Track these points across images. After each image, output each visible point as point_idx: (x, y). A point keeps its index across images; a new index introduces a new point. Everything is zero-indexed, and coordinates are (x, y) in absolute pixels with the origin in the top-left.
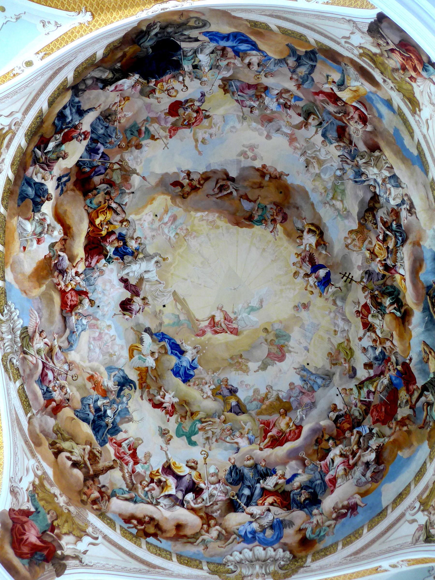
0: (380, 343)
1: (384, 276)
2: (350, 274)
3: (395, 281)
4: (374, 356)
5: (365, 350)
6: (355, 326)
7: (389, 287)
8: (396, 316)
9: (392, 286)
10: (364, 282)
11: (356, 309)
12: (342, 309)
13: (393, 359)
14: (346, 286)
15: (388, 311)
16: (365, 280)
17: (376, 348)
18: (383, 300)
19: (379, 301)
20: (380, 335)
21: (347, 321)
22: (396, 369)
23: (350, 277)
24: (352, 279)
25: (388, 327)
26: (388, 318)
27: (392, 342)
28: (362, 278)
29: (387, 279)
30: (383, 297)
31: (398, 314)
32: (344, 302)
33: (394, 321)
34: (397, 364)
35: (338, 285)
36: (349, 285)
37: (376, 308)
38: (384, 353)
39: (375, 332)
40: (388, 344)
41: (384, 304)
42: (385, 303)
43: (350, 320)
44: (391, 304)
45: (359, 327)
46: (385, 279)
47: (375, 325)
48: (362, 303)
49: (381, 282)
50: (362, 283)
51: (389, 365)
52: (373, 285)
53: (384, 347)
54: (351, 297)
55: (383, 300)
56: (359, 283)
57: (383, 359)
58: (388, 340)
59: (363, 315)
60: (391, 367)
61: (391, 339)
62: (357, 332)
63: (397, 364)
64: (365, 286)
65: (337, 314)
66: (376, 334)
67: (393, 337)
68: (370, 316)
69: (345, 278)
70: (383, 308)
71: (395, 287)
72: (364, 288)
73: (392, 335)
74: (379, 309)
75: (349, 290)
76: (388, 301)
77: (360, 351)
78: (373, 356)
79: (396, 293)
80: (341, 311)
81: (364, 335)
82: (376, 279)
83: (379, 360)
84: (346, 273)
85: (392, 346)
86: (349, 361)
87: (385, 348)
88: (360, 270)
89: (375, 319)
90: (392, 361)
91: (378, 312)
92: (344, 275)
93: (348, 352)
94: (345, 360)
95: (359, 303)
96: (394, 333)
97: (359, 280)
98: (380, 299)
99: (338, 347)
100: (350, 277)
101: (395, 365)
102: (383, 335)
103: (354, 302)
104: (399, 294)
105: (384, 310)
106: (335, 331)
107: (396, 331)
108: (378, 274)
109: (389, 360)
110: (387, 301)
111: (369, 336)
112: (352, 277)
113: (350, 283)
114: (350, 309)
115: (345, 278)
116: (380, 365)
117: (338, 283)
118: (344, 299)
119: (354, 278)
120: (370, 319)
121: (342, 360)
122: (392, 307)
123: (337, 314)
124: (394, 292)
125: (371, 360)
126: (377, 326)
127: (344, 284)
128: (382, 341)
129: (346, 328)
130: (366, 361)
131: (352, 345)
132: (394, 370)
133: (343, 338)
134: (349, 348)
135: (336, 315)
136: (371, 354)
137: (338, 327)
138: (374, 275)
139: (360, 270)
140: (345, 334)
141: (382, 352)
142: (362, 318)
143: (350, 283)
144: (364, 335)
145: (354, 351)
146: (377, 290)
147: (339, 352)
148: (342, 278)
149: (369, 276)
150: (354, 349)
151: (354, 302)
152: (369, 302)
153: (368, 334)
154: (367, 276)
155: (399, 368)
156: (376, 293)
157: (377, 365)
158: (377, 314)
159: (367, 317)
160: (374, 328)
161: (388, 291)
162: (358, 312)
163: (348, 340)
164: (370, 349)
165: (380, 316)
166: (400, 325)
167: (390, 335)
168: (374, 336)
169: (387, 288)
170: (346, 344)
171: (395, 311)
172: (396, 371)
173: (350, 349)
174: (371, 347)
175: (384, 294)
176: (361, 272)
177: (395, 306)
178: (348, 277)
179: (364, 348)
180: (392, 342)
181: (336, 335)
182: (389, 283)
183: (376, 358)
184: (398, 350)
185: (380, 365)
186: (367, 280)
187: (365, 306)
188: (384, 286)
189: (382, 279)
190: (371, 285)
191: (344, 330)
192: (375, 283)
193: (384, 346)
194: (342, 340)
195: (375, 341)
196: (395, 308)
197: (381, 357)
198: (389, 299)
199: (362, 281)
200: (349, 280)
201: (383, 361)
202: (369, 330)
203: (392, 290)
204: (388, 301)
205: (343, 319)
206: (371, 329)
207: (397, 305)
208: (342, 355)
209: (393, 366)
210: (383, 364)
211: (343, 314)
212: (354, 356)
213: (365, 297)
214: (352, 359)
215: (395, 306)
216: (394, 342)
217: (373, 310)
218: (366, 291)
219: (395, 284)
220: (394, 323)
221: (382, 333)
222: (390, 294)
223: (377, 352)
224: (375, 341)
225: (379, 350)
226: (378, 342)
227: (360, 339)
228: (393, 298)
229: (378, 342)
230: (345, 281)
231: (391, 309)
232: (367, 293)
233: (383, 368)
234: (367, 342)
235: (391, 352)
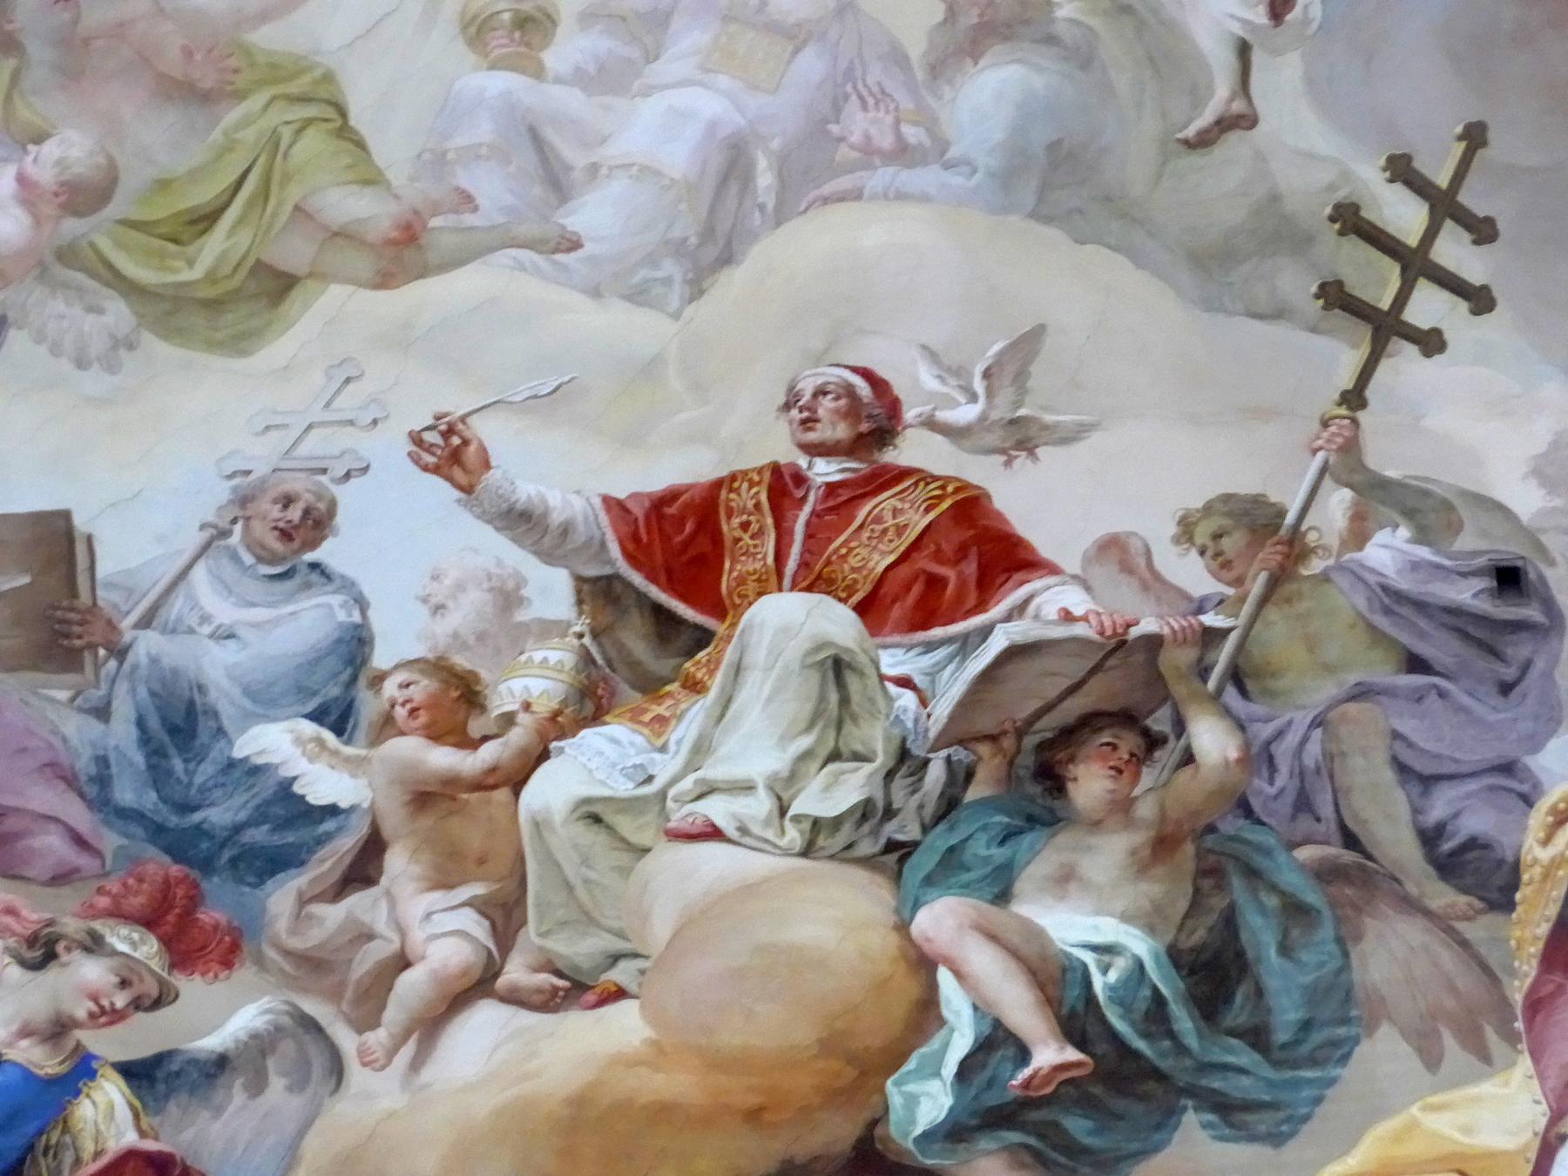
0: (429, 797)
1: (1486, 875)
2: (1480, 300)
3: (1431, 1059)
4: (224, 695)
5: (289, 532)
6: (650, 369)
7: (1318, 952)
8: (893, 1058)
9: (1336, 1022)
10: (1358, 534)
11: (918, 386)
12: (903, 154)
13: (225, 1014)
14: (1275, 230)
15: (942, 919)
16: (1389, 551)
17: (337, 717)
18: (1106, 856)
19: (1090, 784)
20: (552, 790)
21: (713, 233)
22: (83, 1069)
23: (1428, 306)
24: (1386, 328)
25: (700, 921)
26: (838, 920)
27: (480, 984)
28: (1427, 510)
29: (1442, 923)
30: (1163, 845)
31: (923, 1100)
32: (1007, 177)
33: (804, 1034)
34: (142, 1075)
35: (1280, 82)
36: (1296, 284)
37: (958, 733)
38: (277, 862)
39: (589, 703)
40: (437, 928)
41: (1044, 858)
42: (1065, 879)
43: (732, 284)
44: (1060, 986)
45: (632, 439)
46: (1442, 896)
47: (695, 715)
48: (1023, 498)
49: (1393, 835)
50: (1337, 504)
51: (121, 938)
52: (1324, 691)
53: (373, 848)
54: (1091, 299)
55: (1106, 856)
56: (1347, 462)
57: (199, 860)
58: (505, 916)
59: (841, 501)
60: (92, 972)
61: (516, 972)
62: (550, 403)
63: (142, 1075)
64: (1296, 548)
65: (811, 65)
66: (559, 726)
67: (548, 1002)
68: (835, 621)
69: (1405, 216)
70: (980, 848)
71: (1340, 1050)
72: (1254, 534)
73: (575, 989)
74: (959, 778)
75: (1215, 267)
76: (1109, 930)
77: (261, 455)
78: (217, 668)
79: (1246, 1071)
80: (858, 124)
81: (521, 522)
82: (1433, 733)
83: (157, 774)
84: (1483, 231)
85: (411, 986)
86: (67, 255)
87: (363, 870)
88: (1544, 472)
89: (798, 700)
90: (192, 988)
91: (906, 761)
92: (1444, 206)
93: (215, 245)
94: (84, 195)
95: (1021, 439)
96: (624, 1026)
97: (1388, 457)
98: (1122, 807)
99: (278, 71)
100: (1428, 306)
101: (140, 1037)
102: (569, 839)
103: (1027, 345)
104: (1230, 1114)
105: (952, 861)
106: (533, 27)
107: (658, 1055)
108: (1511, 779)
109: (195, 944)
110: (1096, 915)
111: (508, 597)
112: (1431, 342)
113: (1335, 296)
114: (904, 281)
115: (1405, 216)
116: (96, 787)
117: (1319, 90)
118: (1056, 181)
119: (1404, 361)
120: (786, 625)
121: (69, 149)
122: (1022, 1010)
123: (811, 65)
124: (1257, 1037)
125: (147, 645)
126: (685, 732)
127: (1307, 190)
128: (471, 835)
129: (594, 215)
130: (129, 550)
131: (335, 314)
132: (58, 1030)
133: (437, 162)
134: (293, 253)
135: (797, 37)
136: (238, 636)
137: (604, 79)
138: (1487, 708)
139: (1544, 472)
140: (494, 191)
141: (295, 815)
142: (783, 486)
143: (1335, 296)
144: (521, 522)
145: (240, 343)
146: (1259, 758)
147: (194, 92)
148: (1402, 170)
149: (1456, 619)
150: (279, 350)
151: (1027, 345)
152: (1052, 607)
153: (551, 592)
154: (1468, 594)
155: (106, 1115)
156: (1212, 740)
157: (78, 731)
158: (876, 737)
159: (815, 581)
160: (651, 686)
161: (1260, 932)
162: (875, 417)
163: (404, 253)
164: (307, 622)
165: (845, 790)
166: (754, 1116)
167: (579, 949)
168: (531, 682)
169: (1296, 911)
170: (348, 204)
171: (961, 1042)
172: (42, 1060)
173: (275, 287)
174: (355, 645)
175: (1206, 855)
176: (1526, 501)
177: (1049, 1053)
178: (1416, 264)
179: (316, 523)
180: (480, 984)
181: (477, 31)
182: (1393, 954)
183: (180, 723)
184: (373, 1094)
185: (96, 787)
186: (1392, 599)
187: (1001, 558)
188: (1326, 874)
189: (1430, 838)
190: (1320, 660)
191: (558, 183)
192: (1365, 731)
193: (398, 862)
194: (393, 148)
195: (457, 701)
196: (998, 1042)
197: (219, 815)
198: (1139, 944)
199: (1380, 497)
200: (1378, 281)
201: (157, 832)
202: (600, 593)
203: (1286, 1014)
204: (1109, 930)
205: (732, 161)
206: (636, 639)
207: (1067, 1089)
208: (162, 149)
209: (107, 1016)
210: (110, 841)
211: (815, 171)
212: (151, 343)
213: (1116, 551)
214: (118, 313)
215: (1049, 1053)
216: (483, 1030)
217: (926, 680)
218: (1222, 565)
219: (1383, 1053)
220: (773, 1026)
221: (592, 815)
222: (1213, 971)
223: (279, 743)
224: (457, 701)
225: (326, 782)
226: (443, 758)
227: (451, 454)
228: (1156, 1016)
229: (443, 758)
230: (1352, 221)
231: (982, 984)
232: (1191, 574)
233: (52, 844)
234: (414, 571)
235: (314, 966)
